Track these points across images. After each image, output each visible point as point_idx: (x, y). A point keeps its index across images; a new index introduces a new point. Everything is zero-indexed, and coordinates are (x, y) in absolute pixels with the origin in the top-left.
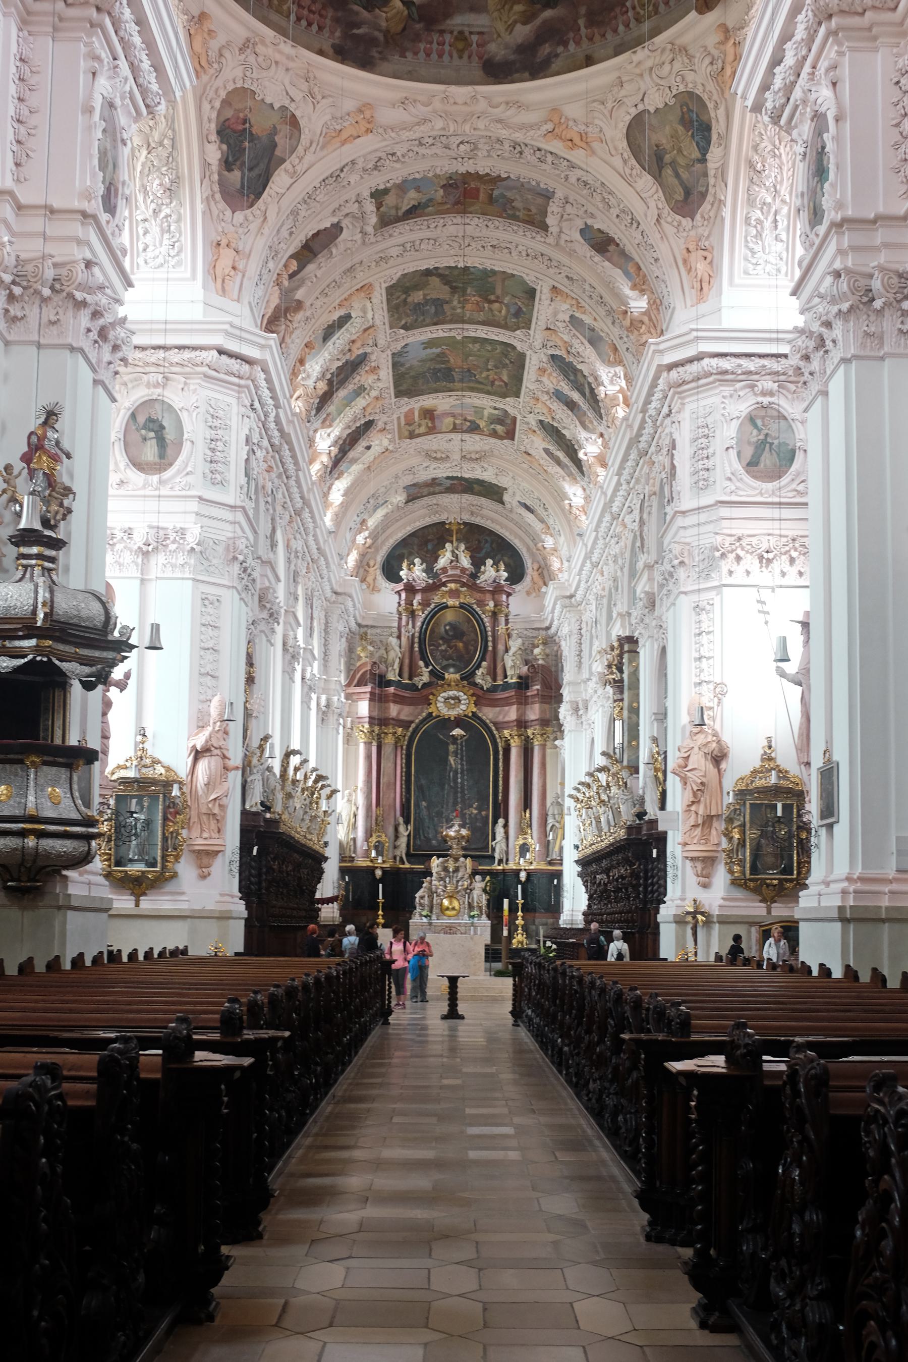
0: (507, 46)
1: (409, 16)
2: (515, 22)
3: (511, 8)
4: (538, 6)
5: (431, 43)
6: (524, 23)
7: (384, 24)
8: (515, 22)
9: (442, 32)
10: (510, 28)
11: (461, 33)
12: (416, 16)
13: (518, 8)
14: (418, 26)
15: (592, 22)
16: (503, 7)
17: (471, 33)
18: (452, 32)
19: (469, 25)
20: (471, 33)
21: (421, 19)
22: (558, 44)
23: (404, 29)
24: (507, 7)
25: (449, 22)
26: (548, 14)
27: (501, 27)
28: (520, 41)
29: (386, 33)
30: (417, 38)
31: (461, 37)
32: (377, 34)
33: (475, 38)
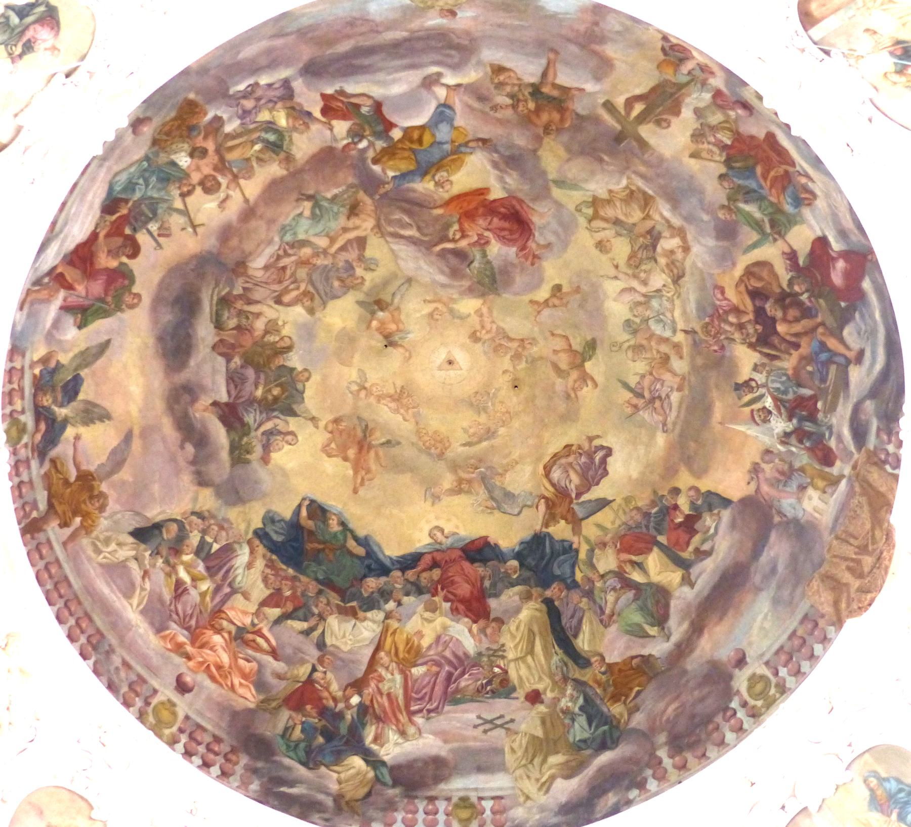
0: (542, 809)
1: (377, 779)
2: (553, 778)
3: (544, 761)
4: (588, 752)
5: (416, 812)
6: (568, 777)
7: (334, 787)
8: (553, 778)
9: (432, 799)
10: (546, 787)
11: (464, 799)
12: (388, 779)
13: (556, 759)
14: (391, 792)
15: (678, 745)
16: (531, 762)
17: (480, 799)
18: (448, 799)
19: (476, 789)
20: (480, 799)
21: (396, 783)
22: (629, 788)
23: (369, 794)
24: (537, 761)
25: (442, 786)
26: (606, 757)
27: (530, 787)
28: (563, 799)
29: (338, 798)
30: (391, 806)
31: (464, 802)
32: (321, 797)
33: (488, 805)
